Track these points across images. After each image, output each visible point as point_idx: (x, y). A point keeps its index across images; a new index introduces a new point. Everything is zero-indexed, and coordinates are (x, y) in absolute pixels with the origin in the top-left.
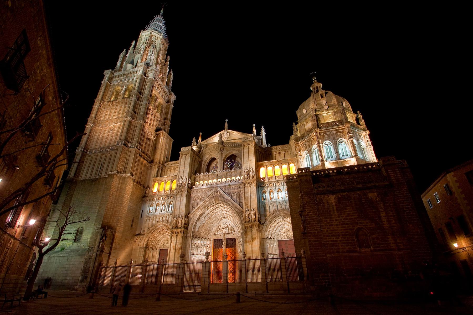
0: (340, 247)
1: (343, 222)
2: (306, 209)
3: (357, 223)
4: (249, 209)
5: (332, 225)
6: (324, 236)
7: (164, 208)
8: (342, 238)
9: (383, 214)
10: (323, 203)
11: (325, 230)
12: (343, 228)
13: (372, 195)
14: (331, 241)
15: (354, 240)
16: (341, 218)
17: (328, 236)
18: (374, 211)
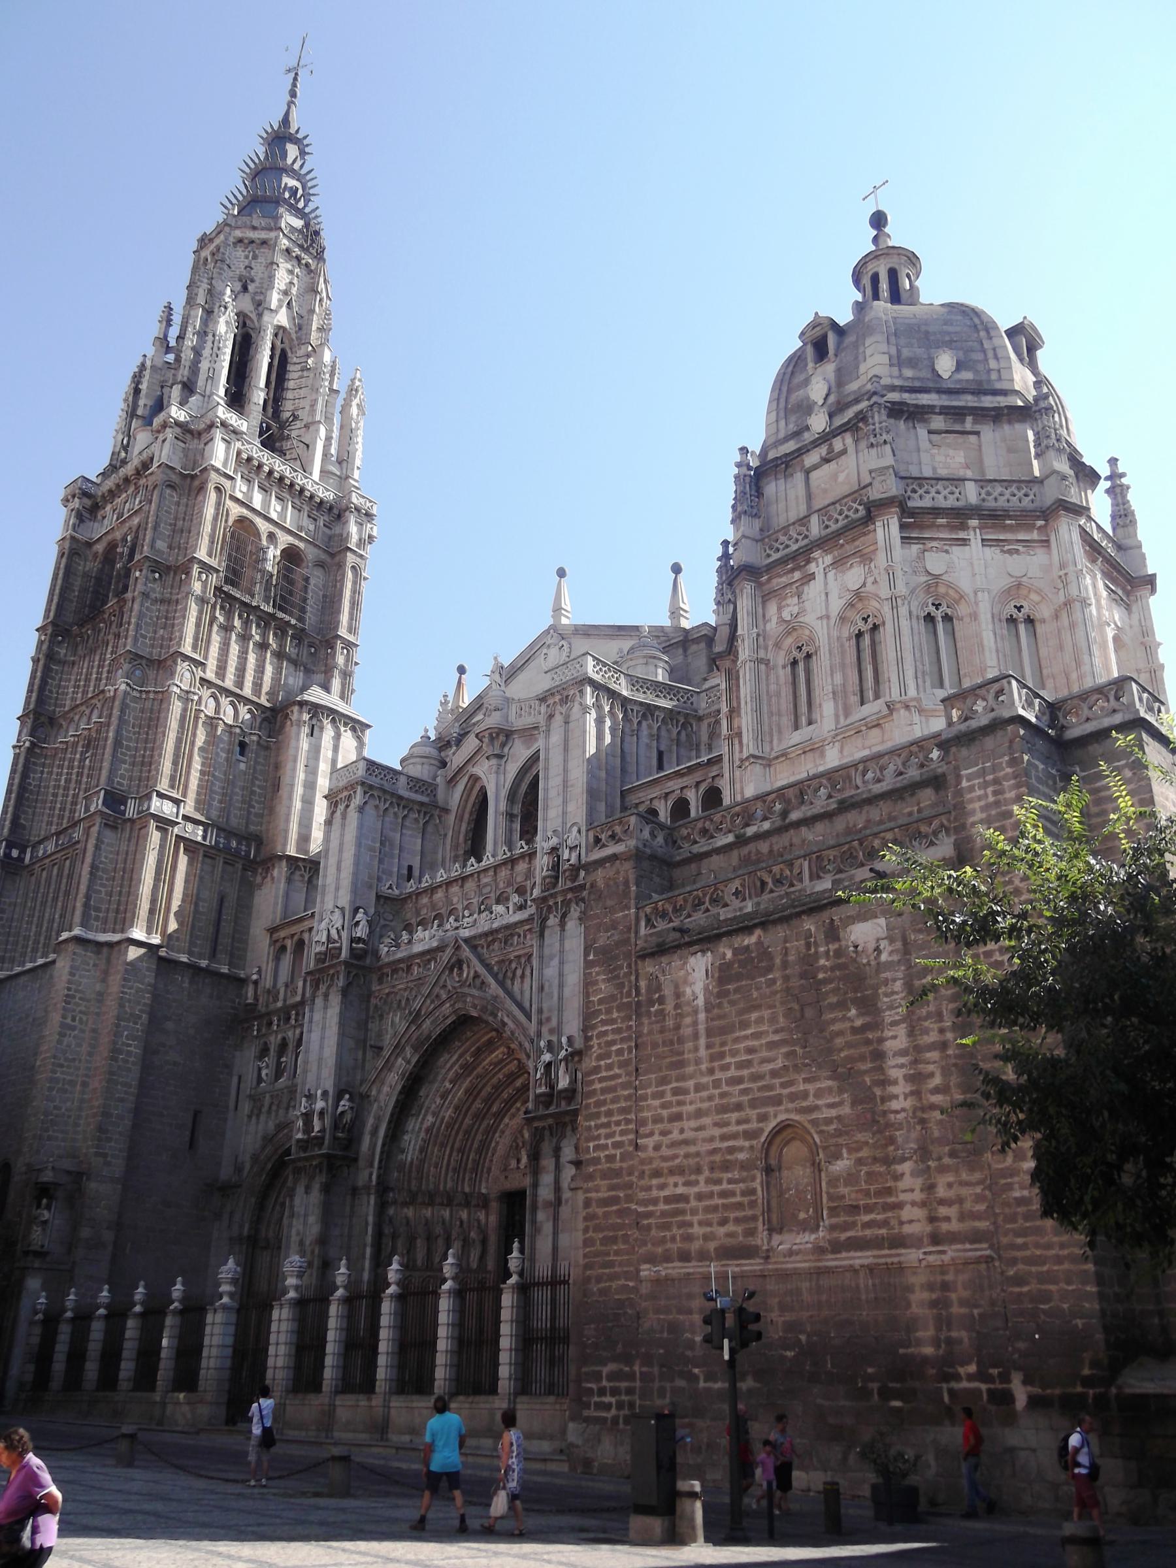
0: (697, 1230)
1: (723, 1095)
2: (595, 1041)
3: (777, 1101)
4: (554, 1039)
5: (677, 1117)
6: (642, 1175)
8: (709, 1181)
9: (896, 1040)
10: (661, 1001)
11: (650, 1142)
12: (717, 1132)
13: (865, 934)
14: (667, 1200)
15: (753, 1192)
16: (719, 1075)
17: (657, 1173)
18: (858, 1023)
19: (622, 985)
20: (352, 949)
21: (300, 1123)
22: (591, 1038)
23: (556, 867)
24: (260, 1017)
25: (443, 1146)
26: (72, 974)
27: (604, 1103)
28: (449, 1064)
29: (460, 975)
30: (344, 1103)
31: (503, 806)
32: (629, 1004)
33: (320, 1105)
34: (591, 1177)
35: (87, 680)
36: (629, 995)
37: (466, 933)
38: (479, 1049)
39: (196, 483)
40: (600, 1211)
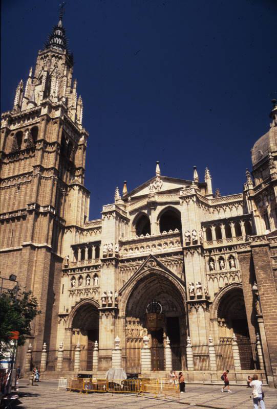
7: (88, 282)
19: (269, 275)
20: (116, 255)
21: (104, 299)
22: (260, 287)
23: (190, 240)
24: (71, 269)
25: (137, 306)
26: (30, 255)
27: (268, 302)
28: (142, 285)
29: (151, 264)
30: (116, 295)
31: (156, 221)
32: (272, 280)
33: (111, 295)
34: (266, 320)
35: (14, 169)
36: (272, 277)
37: (152, 254)
38: (151, 282)
39: (54, 121)
40: (271, 327)
